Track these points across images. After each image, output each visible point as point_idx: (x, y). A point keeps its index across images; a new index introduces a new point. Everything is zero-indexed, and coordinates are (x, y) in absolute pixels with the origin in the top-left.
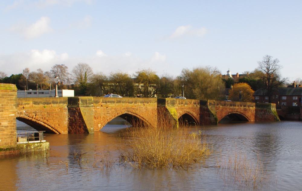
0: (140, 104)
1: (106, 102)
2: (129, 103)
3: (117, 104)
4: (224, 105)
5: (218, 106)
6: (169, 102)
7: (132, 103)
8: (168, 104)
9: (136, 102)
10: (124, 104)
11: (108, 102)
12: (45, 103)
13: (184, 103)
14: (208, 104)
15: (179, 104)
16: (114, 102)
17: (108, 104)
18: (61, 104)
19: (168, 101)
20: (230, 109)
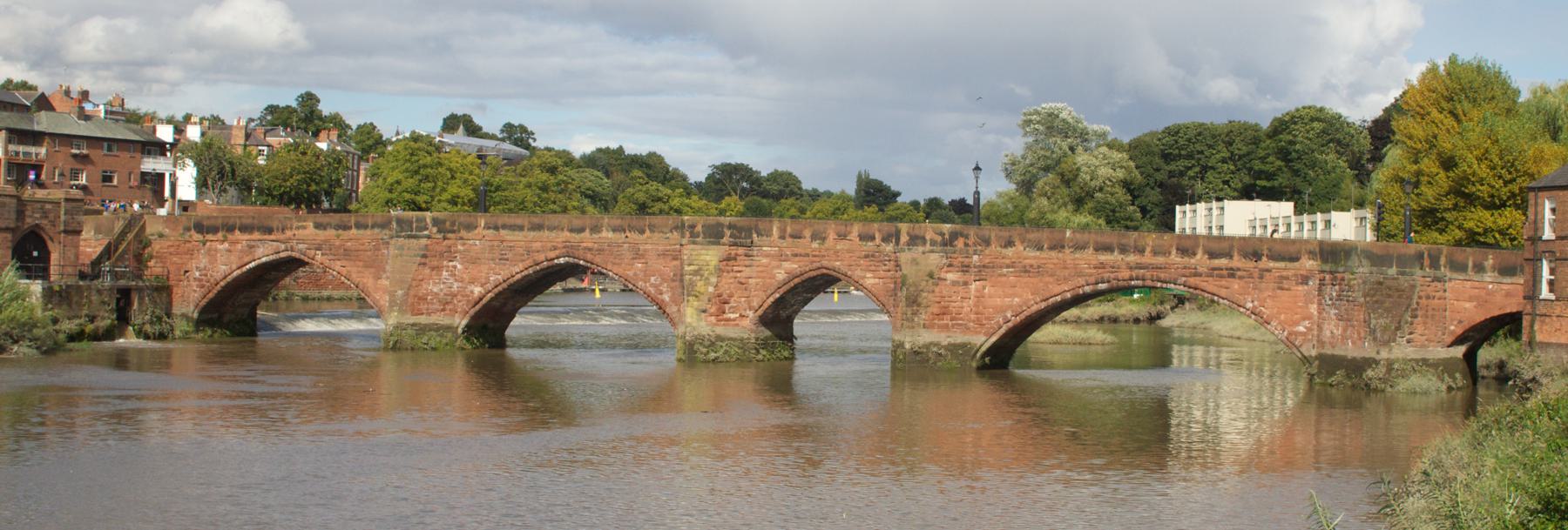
0: (610, 235)
1: (496, 228)
2: (571, 231)
3: (532, 234)
4: (1051, 248)
5: (1010, 251)
6: (699, 228)
7: (582, 230)
8: (693, 235)
9: (596, 229)
10: (553, 234)
11: (504, 227)
12: (338, 227)
13: (807, 233)
14: (904, 238)
15: (782, 237)
16: (521, 228)
17: (503, 232)
18: (377, 230)
19: (693, 227)
20: (1102, 266)
